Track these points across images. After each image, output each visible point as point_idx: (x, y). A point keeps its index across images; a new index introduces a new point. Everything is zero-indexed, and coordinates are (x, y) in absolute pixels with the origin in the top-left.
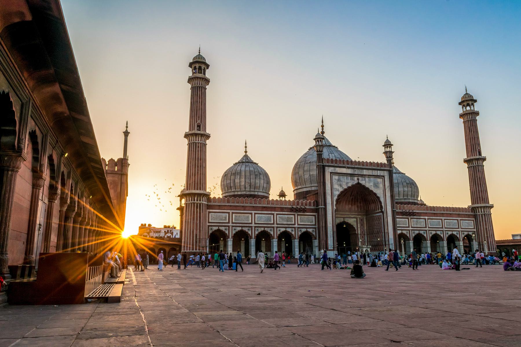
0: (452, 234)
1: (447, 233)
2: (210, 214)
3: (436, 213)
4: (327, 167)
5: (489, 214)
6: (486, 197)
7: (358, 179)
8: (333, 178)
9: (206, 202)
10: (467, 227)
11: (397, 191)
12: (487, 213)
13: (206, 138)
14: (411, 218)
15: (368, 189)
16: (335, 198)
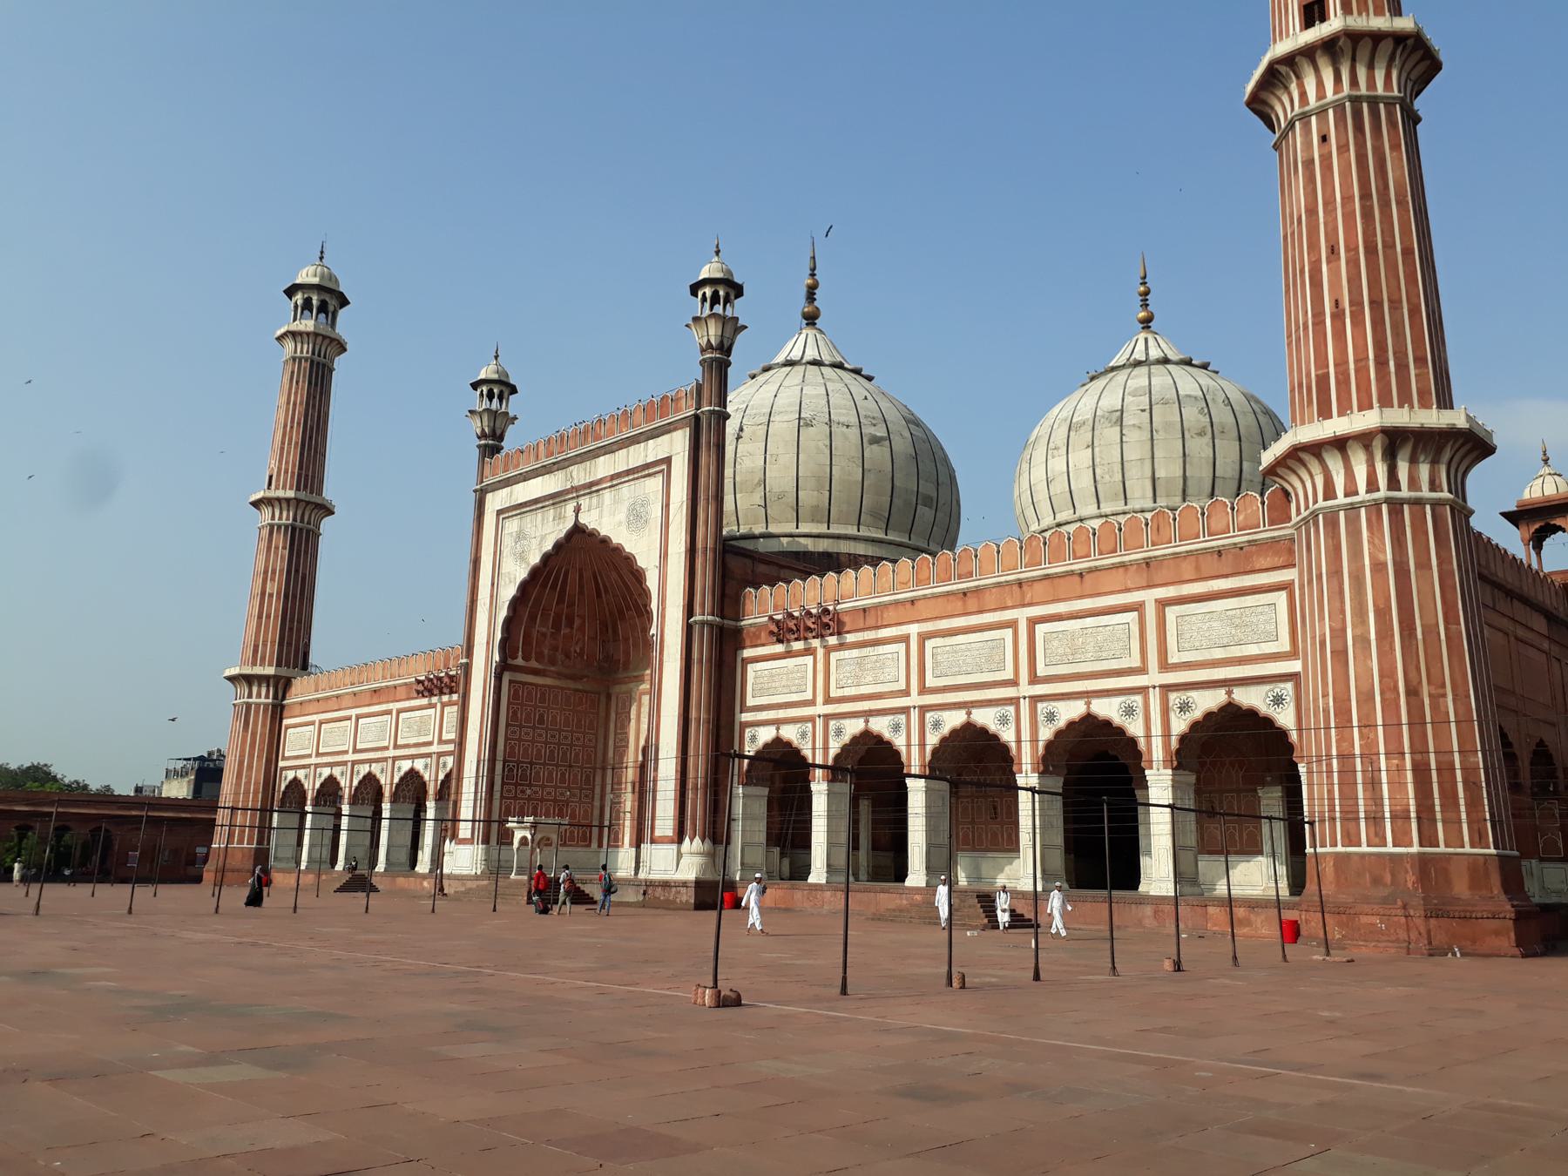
0: (1089, 719)
1: (1051, 717)
2: (289, 731)
3: (978, 591)
4: (491, 494)
5: (1352, 509)
6: (1341, 363)
7: (577, 510)
8: (506, 531)
9: (267, 697)
10: (1219, 654)
11: (1026, 490)
12: (1341, 499)
13: (284, 505)
14: (828, 650)
15: (605, 541)
16: (503, 614)
